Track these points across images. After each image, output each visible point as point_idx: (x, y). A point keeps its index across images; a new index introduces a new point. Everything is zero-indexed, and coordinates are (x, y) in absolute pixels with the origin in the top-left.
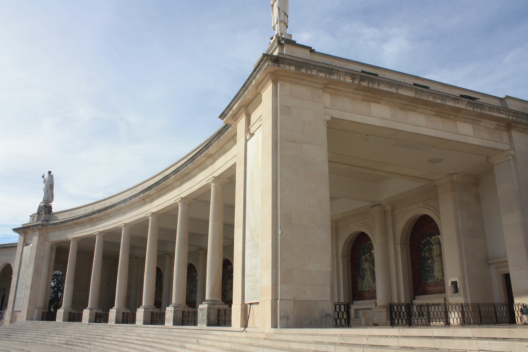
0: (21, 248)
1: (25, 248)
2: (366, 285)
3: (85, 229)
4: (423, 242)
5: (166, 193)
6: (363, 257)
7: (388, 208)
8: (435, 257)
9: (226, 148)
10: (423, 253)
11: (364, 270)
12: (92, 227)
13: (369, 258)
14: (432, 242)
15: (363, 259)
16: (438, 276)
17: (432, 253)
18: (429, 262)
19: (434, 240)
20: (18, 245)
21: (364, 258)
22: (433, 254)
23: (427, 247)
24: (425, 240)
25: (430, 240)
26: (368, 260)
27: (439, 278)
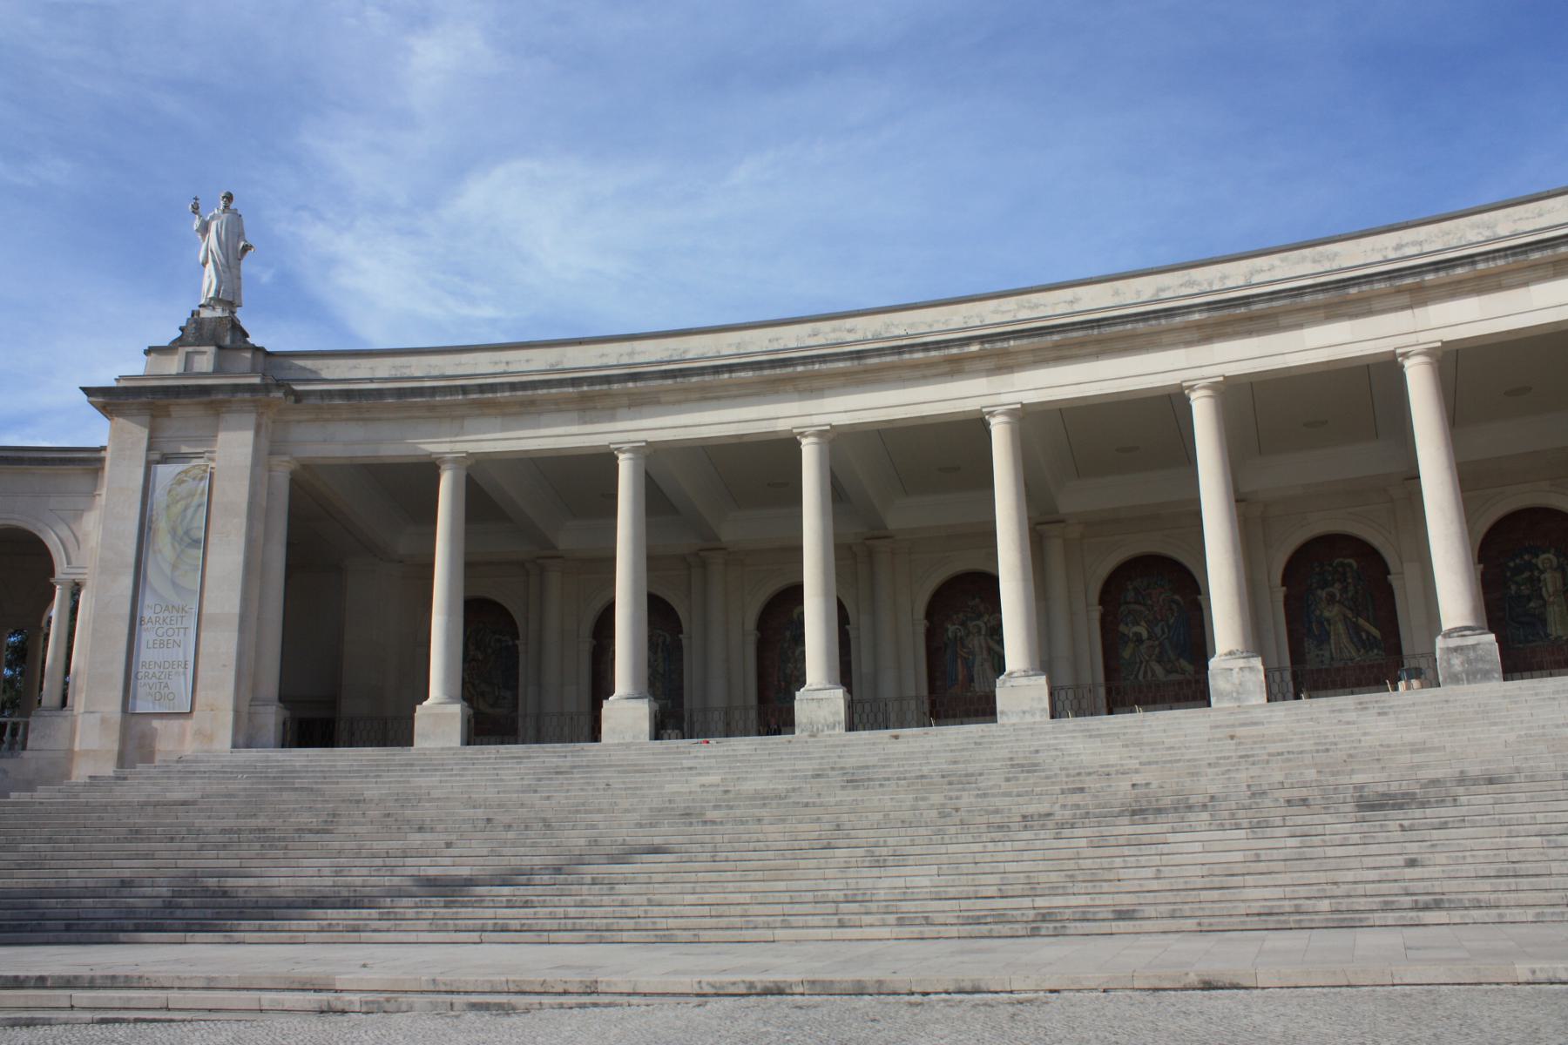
0: (140, 472)
1: (165, 473)
2: (1334, 655)
3: (539, 426)
4: (1512, 564)
6: (1323, 594)
8: (1550, 596)
10: (1513, 588)
11: (1325, 623)
12: (503, 430)
13: (1341, 595)
14: (1540, 566)
16: (1560, 633)
17: (1541, 589)
18: (1532, 604)
19: (1546, 561)
20: (107, 455)
21: (1324, 595)
22: (1544, 589)
23: (1527, 574)
24: (1518, 561)
26: (1337, 599)
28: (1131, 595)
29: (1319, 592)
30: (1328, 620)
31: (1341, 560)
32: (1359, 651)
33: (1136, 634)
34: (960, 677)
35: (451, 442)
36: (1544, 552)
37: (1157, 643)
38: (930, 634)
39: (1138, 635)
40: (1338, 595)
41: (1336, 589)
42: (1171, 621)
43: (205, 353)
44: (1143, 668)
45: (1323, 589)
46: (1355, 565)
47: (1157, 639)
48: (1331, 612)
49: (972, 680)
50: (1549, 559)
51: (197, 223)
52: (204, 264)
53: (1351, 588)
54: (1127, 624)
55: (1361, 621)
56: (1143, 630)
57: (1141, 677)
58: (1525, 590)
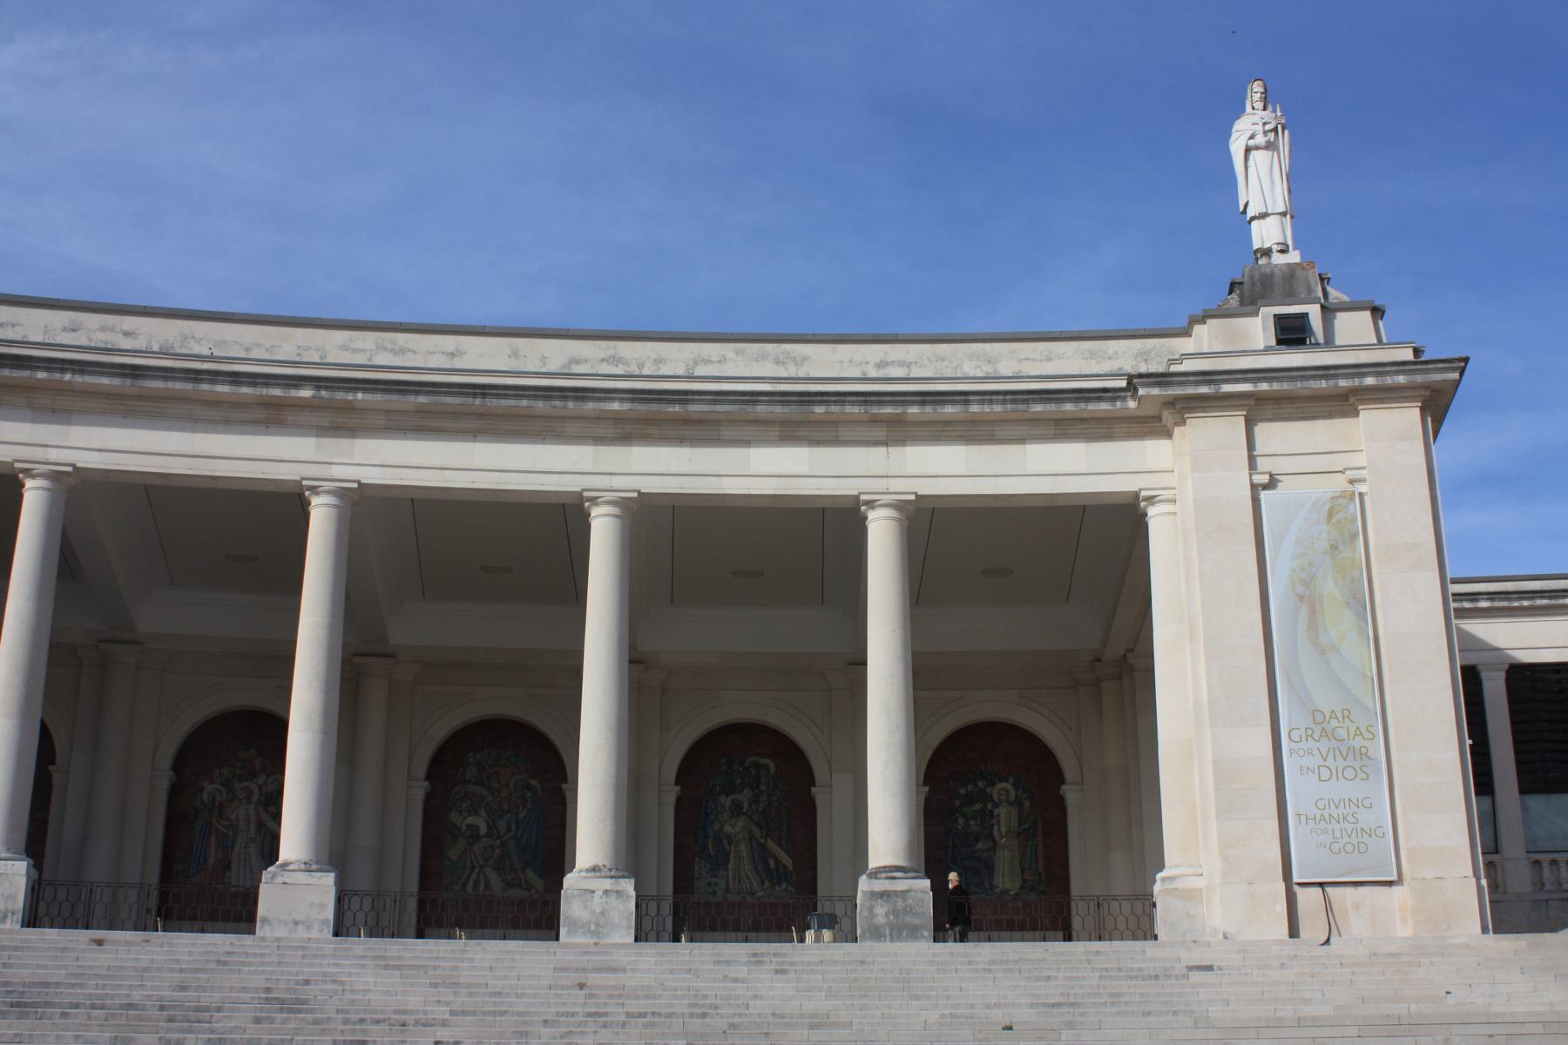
2: (731, 886)
4: (962, 791)
5: (475, 434)
6: (726, 801)
8: (1002, 837)
9: (994, 430)
10: (961, 821)
11: (725, 841)
13: (750, 806)
14: (995, 797)
16: (1008, 886)
17: (992, 826)
18: (980, 845)
19: (1002, 792)
21: (728, 804)
22: (996, 828)
23: (978, 806)
24: (970, 787)
25: (989, 790)
26: (744, 810)
27: (1009, 891)
29: (723, 798)
30: (728, 837)
31: (755, 758)
32: (763, 883)
33: (470, 826)
34: (212, 860)
36: (1001, 781)
37: (498, 842)
39: (474, 829)
40: (746, 805)
41: (744, 797)
42: (522, 815)
44: (474, 876)
47: (499, 837)
48: (735, 827)
49: (227, 866)
50: (1007, 790)
53: (764, 798)
54: (460, 812)
55: (771, 844)
57: (469, 889)
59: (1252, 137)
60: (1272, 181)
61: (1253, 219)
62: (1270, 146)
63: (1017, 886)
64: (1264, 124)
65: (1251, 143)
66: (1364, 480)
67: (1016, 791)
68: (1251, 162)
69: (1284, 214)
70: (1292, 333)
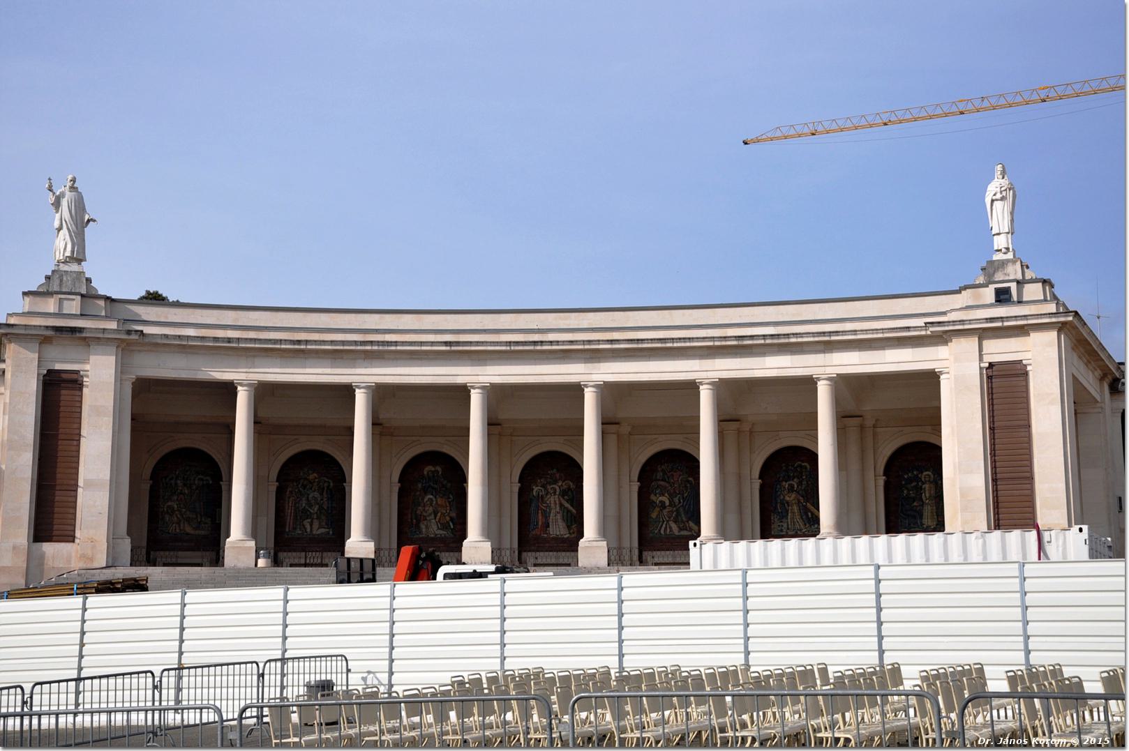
2: (790, 526)
4: (906, 477)
7: (869, 422)
13: (798, 487)
14: (923, 479)
15: (785, 488)
16: (930, 524)
18: (915, 504)
21: (787, 486)
23: (914, 484)
25: (919, 476)
28: (660, 475)
29: (784, 483)
30: (788, 503)
31: (799, 463)
32: (805, 525)
33: (661, 502)
34: (540, 523)
35: (246, 372)
36: (926, 471)
37: (675, 509)
38: (521, 493)
39: (662, 503)
40: (796, 486)
41: (795, 483)
43: (74, 300)
44: (664, 526)
45: (786, 482)
46: (808, 467)
47: (675, 506)
48: (791, 498)
51: (52, 199)
52: (60, 229)
53: (804, 482)
54: (656, 495)
56: (665, 499)
57: (662, 532)
58: (912, 494)
59: (995, 195)
60: (1003, 217)
61: (994, 235)
62: (1003, 199)
63: (935, 523)
64: (1001, 187)
65: (994, 198)
66: (1030, 365)
67: (934, 475)
68: (994, 207)
69: (1008, 233)
70: (1003, 297)
